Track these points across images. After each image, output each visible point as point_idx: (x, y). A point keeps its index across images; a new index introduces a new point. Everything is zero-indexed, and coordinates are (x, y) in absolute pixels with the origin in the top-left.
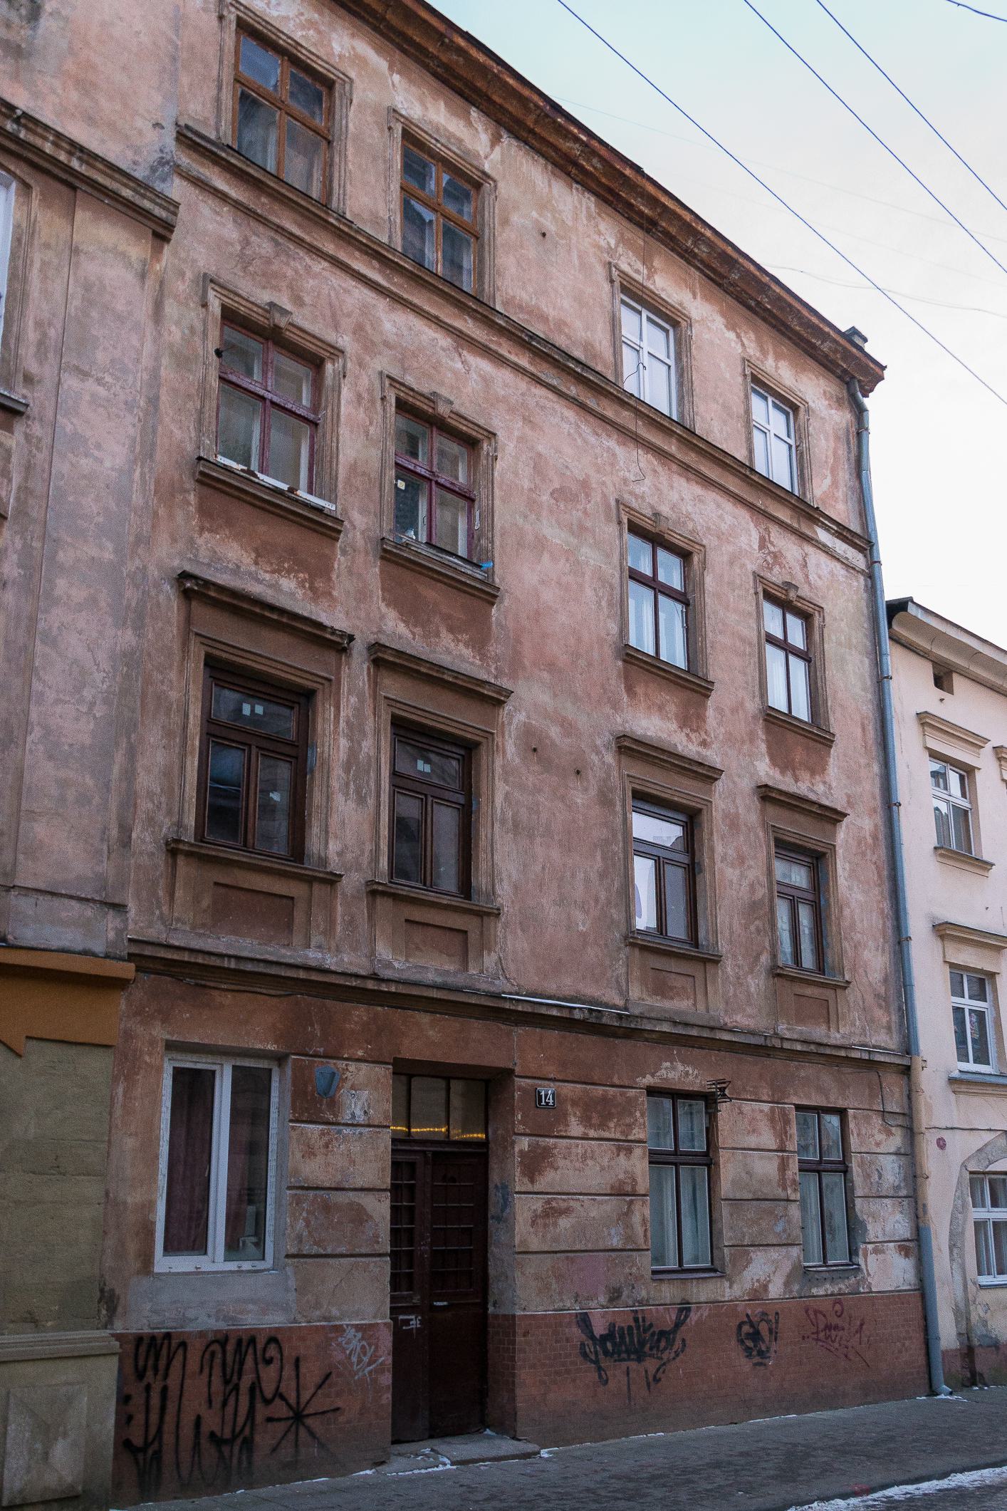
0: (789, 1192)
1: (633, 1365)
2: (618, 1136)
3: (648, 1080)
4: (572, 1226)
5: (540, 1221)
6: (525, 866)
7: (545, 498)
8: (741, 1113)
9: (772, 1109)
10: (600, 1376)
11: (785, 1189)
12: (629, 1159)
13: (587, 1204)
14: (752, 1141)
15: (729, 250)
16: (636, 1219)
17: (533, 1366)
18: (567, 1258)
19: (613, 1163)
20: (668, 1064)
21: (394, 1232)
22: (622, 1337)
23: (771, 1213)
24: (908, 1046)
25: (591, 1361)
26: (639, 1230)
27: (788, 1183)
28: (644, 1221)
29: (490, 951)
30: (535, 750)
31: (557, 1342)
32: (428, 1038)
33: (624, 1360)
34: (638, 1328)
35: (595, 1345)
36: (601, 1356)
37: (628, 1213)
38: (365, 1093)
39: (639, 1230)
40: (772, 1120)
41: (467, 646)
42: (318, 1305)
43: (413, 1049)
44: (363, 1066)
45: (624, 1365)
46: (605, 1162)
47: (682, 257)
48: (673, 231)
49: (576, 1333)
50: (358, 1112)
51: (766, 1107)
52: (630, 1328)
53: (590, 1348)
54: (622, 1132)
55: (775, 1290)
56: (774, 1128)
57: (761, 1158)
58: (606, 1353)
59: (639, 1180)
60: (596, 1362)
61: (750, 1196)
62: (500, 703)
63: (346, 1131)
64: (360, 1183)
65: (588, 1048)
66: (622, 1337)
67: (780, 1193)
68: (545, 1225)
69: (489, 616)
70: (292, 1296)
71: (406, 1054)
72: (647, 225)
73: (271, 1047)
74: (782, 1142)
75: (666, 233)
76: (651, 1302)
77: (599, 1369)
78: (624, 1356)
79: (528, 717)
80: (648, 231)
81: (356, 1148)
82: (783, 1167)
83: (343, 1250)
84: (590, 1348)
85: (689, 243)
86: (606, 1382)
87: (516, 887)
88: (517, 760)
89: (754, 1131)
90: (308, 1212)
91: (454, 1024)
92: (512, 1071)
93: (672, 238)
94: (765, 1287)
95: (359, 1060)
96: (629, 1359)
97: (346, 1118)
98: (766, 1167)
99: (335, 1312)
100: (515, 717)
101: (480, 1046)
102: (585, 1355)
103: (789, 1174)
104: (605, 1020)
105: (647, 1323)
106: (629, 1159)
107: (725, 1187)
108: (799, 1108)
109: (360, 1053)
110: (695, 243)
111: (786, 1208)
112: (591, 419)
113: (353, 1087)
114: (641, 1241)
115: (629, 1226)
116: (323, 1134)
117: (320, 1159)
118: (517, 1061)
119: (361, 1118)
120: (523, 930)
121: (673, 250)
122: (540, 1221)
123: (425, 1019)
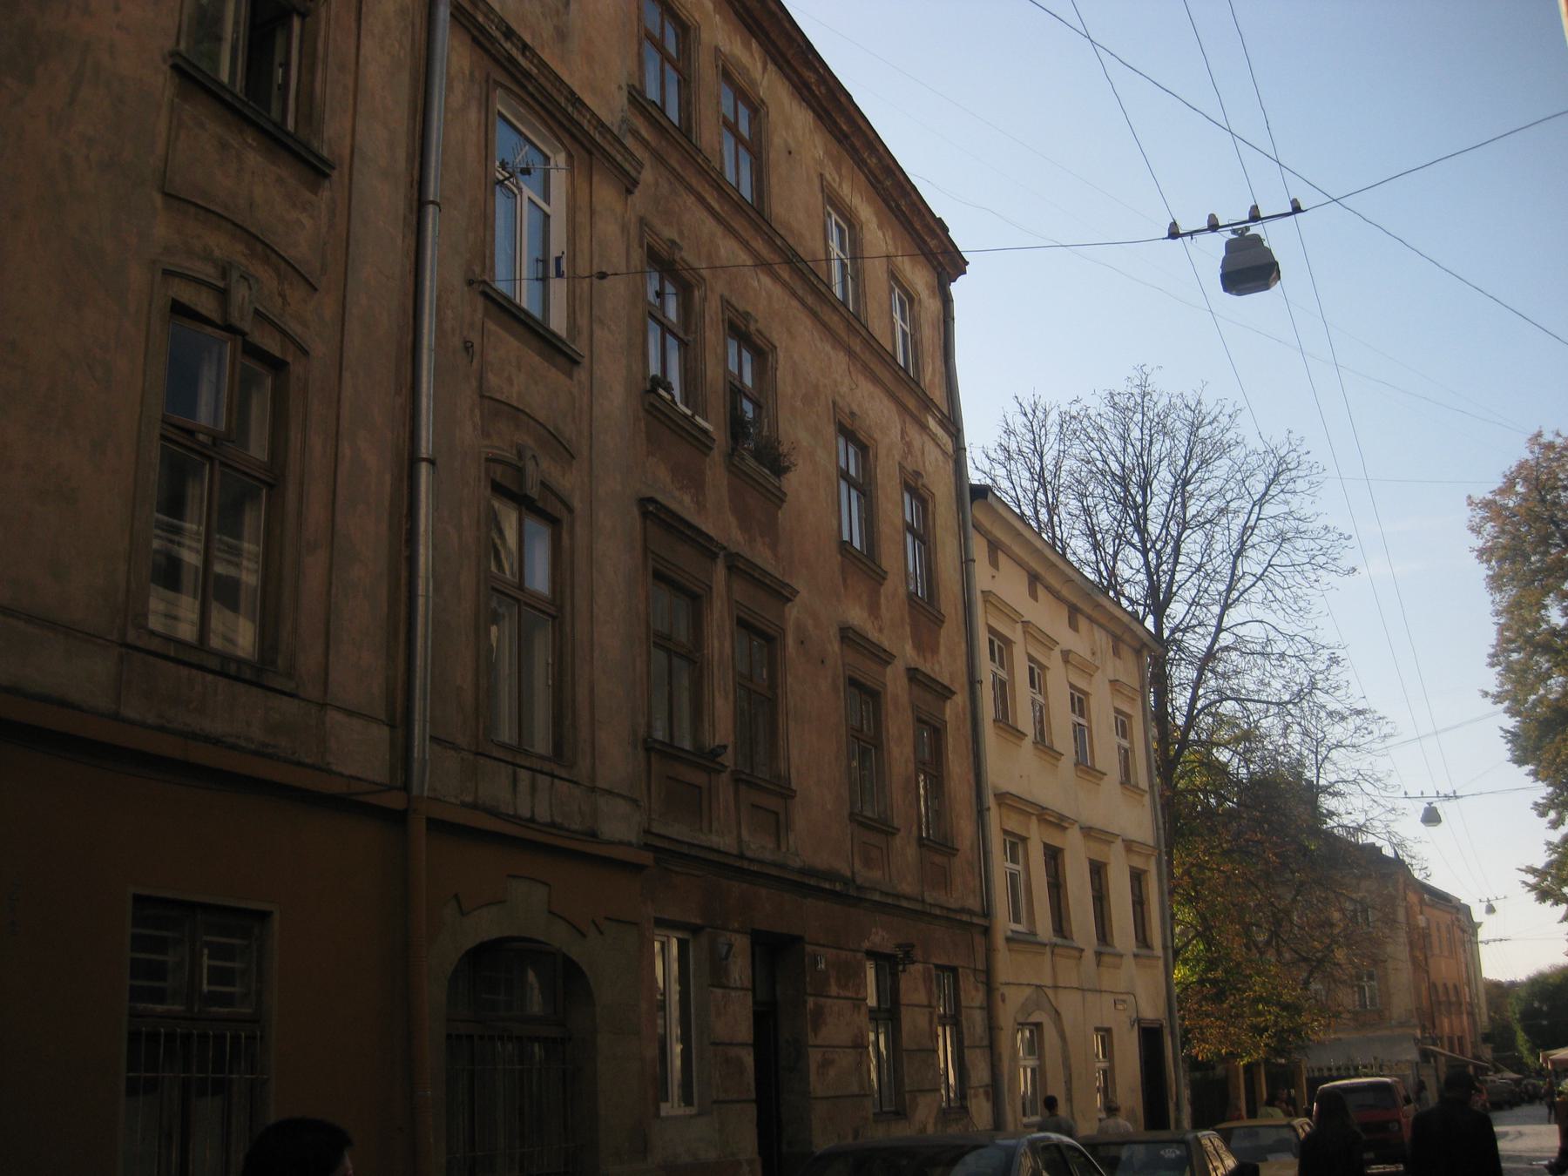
3: (866, 945)
7: (799, 404)
21: (757, 1080)
24: (987, 913)
48: (858, 144)
55: (930, 1129)
62: (789, 600)
72: (841, 137)
80: (840, 142)
94: (925, 1128)
100: (793, 612)
108: (937, 966)
119: (738, 984)
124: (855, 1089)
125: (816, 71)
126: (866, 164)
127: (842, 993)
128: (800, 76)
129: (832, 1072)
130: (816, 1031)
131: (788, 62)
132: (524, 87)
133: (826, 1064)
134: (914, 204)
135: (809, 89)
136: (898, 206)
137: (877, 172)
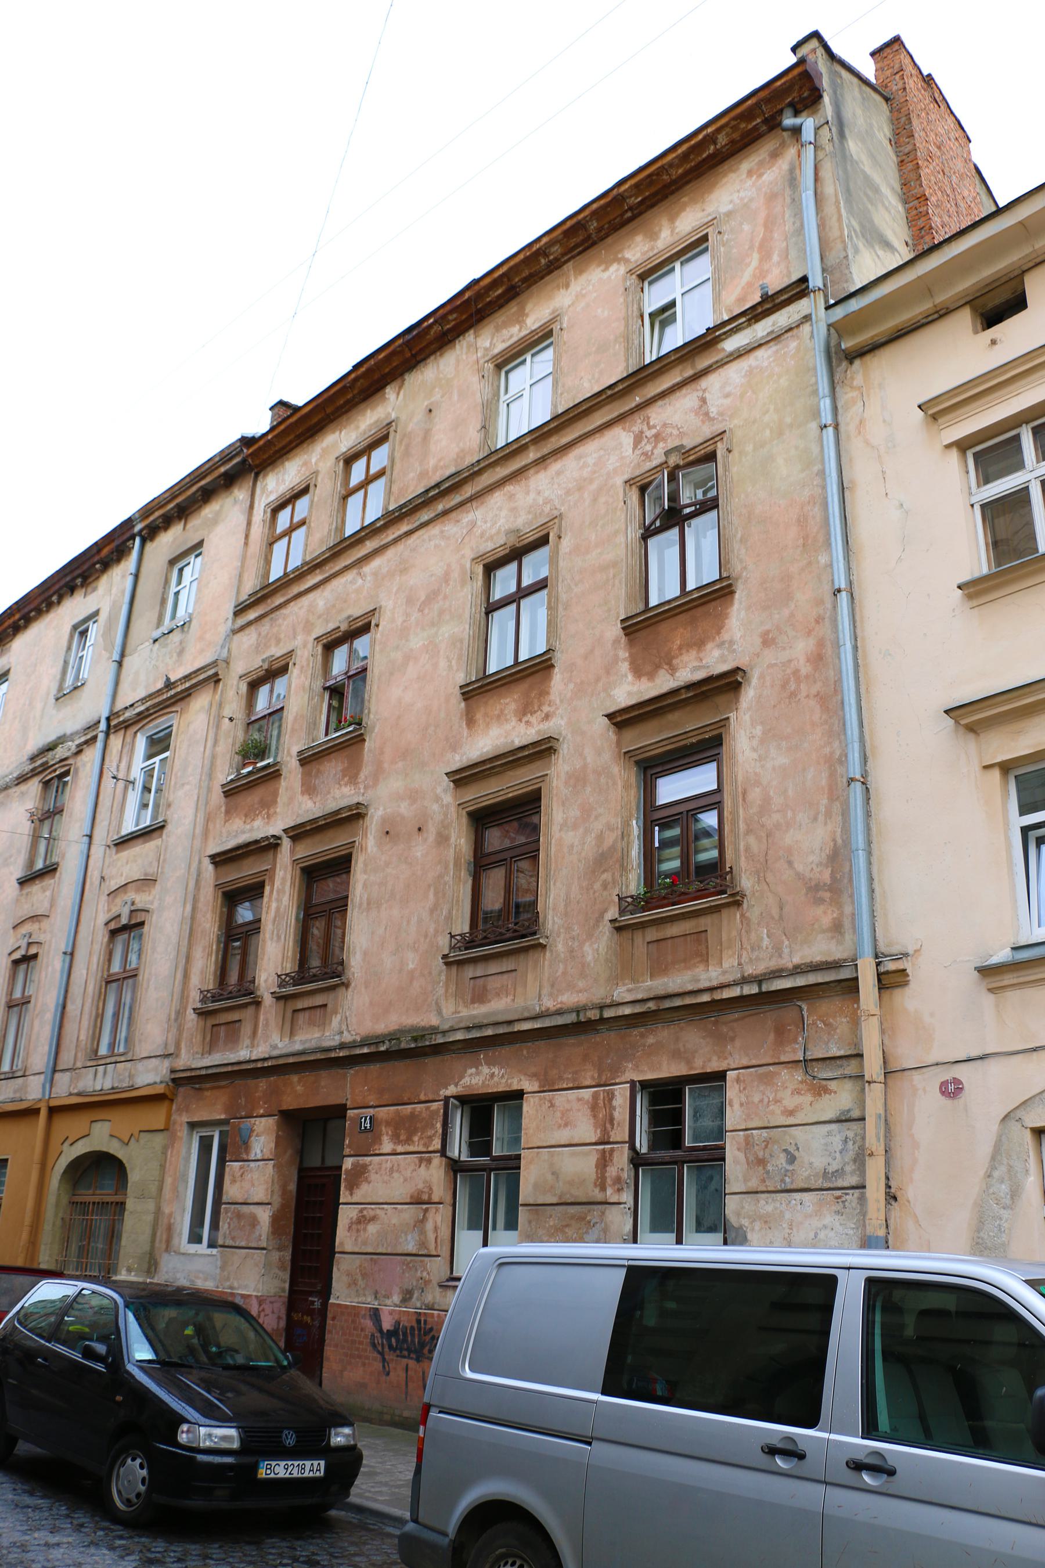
0: (609, 1191)
1: (412, 1363)
2: (421, 1149)
4: (378, 1232)
5: (354, 1226)
6: (373, 933)
8: (552, 1105)
9: (595, 1096)
10: (384, 1366)
11: (603, 1189)
12: (428, 1168)
13: (389, 1212)
14: (563, 1136)
15: (569, 224)
16: (429, 1226)
17: (336, 1346)
18: (371, 1259)
19: (414, 1174)
20: (473, 1070)
22: (405, 1334)
23: (582, 1218)
25: (378, 1352)
26: (431, 1236)
27: (609, 1181)
28: (436, 1229)
29: (336, 1013)
30: (387, 833)
31: (355, 1329)
32: (299, 1093)
33: (404, 1357)
34: (420, 1329)
35: (382, 1338)
36: (386, 1349)
37: (423, 1221)
38: (263, 1136)
39: (431, 1236)
40: (594, 1107)
41: (346, 785)
42: (228, 1279)
43: (289, 1103)
44: (263, 1120)
45: (405, 1361)
46: (408, 1174)
47: (551, 272)
48: (526, 273)
49: (368, 1323)
50: (258, 1152)
51: (587, 1094)
52: (412, 1328)
53: (378, 1340)
54: (425, 1145)
56: (595, 1116)
57: (573, 1154)
58: (390, 1347)
59: (435, 1188)
60: (382, 1354)
61: (554, 1200)
63: (252, 1164)
64: (256, 1200)
65: (400, 1073)
66: (405, 1334)
67: (598, 1196)
68: (358, 1231)
69: (363, 749)
70: (218, 1271)
71: (285, 1107)
73: (223, 1117)
74: (605, 1131)
75: (525, 280)
76: (436, 1307)
77: (384, 1360)
78: (406, 1353)
79: (385, 809)
81: (255, 1177)
82: (604, 1161)
83: (243, 1244)
84: (378, 1340)
85: (543, 261)
86: (388, 1374)
87: (365, 954)
88: (375, 849)
89: (566, 1125)
90: (231, 1219)
91: (309, 1077)
92: (345, 1105)
93: (531, 275)
95: (261, 1116)
96: (409, 1357)
97: (252, 1157)
98: (580, 1166)
99: (236, 1285)
101: (325, 1090)
102: (374, 1345)
103: (612, 1171)
104: (403, 1045)
105: (428, 1327)
106: (428, 1168)
107: (526, 1193)
109: (262, 1111)
110: (546, 255)
111: (603, 1213)
112: (453, 515)
113: (257, 1136)
114: (432, 1246)
115: (423, 1232)
116: (241, 1168)
117: (238, 1185)
118: (349, 1097)
119: (259, 1157)
120: (366, 987)
121: (542, 278)
122: (354, 1226)
123: (295, 1078)
124: (411, 1247)
125: (430, 326)
126: (556, 259)
127: (400, 1149)
128: (431, 343)
129: (372, 1228)
130: (351, 1188)
131: (414, 356)
132: (151, 714)
133: (362, 1221)
134: (637, 186)
135: (444, 334)
136: (631, 209)
137: (573, 242)
